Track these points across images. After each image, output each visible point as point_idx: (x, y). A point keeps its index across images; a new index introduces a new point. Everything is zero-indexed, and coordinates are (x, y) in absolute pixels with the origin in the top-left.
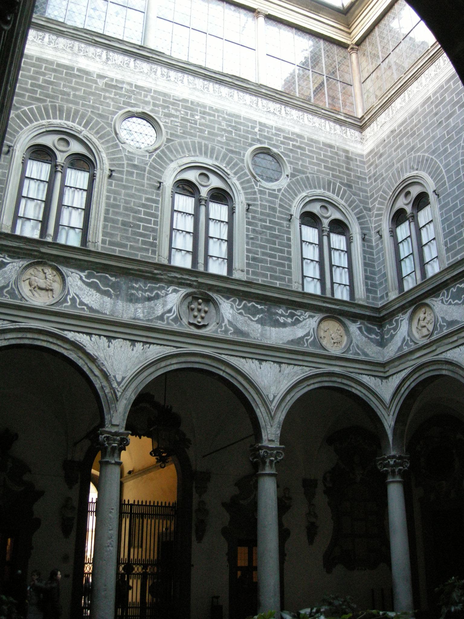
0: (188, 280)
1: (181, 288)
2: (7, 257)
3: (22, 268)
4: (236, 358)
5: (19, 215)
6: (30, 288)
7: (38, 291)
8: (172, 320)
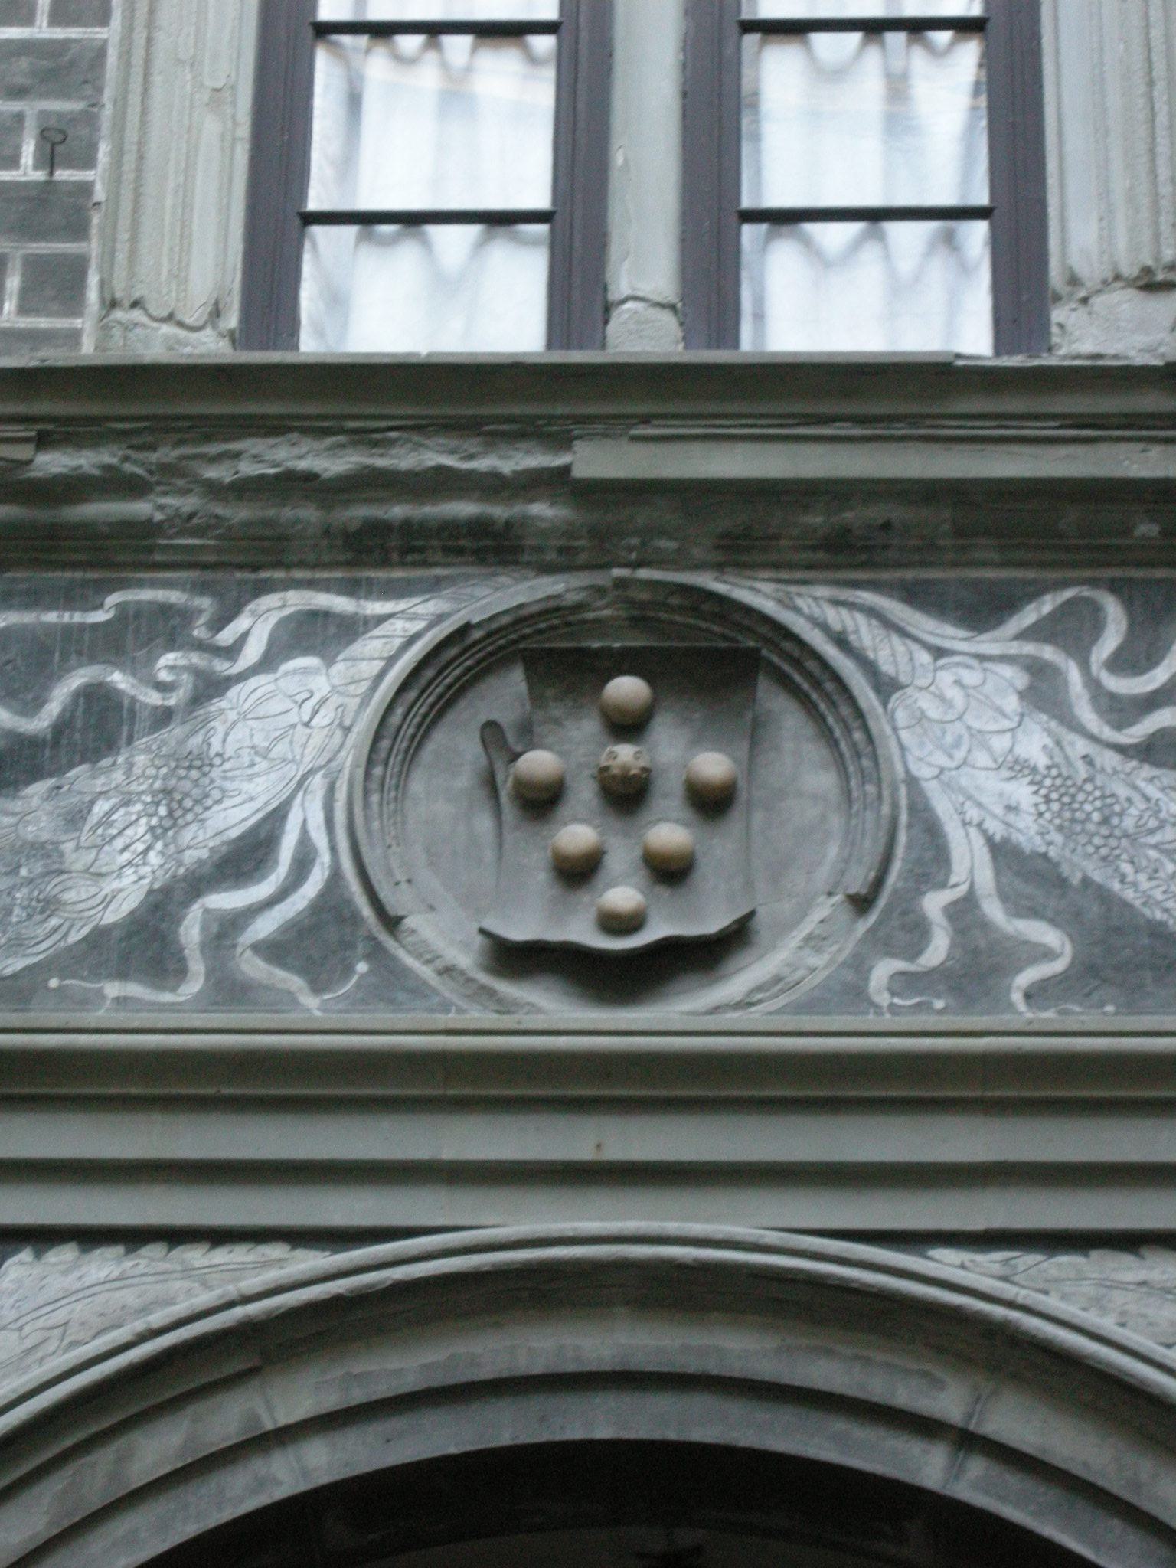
0: (442, 483)
1: (391, 591)
4: (1125, 1268)
8: (274, 950)
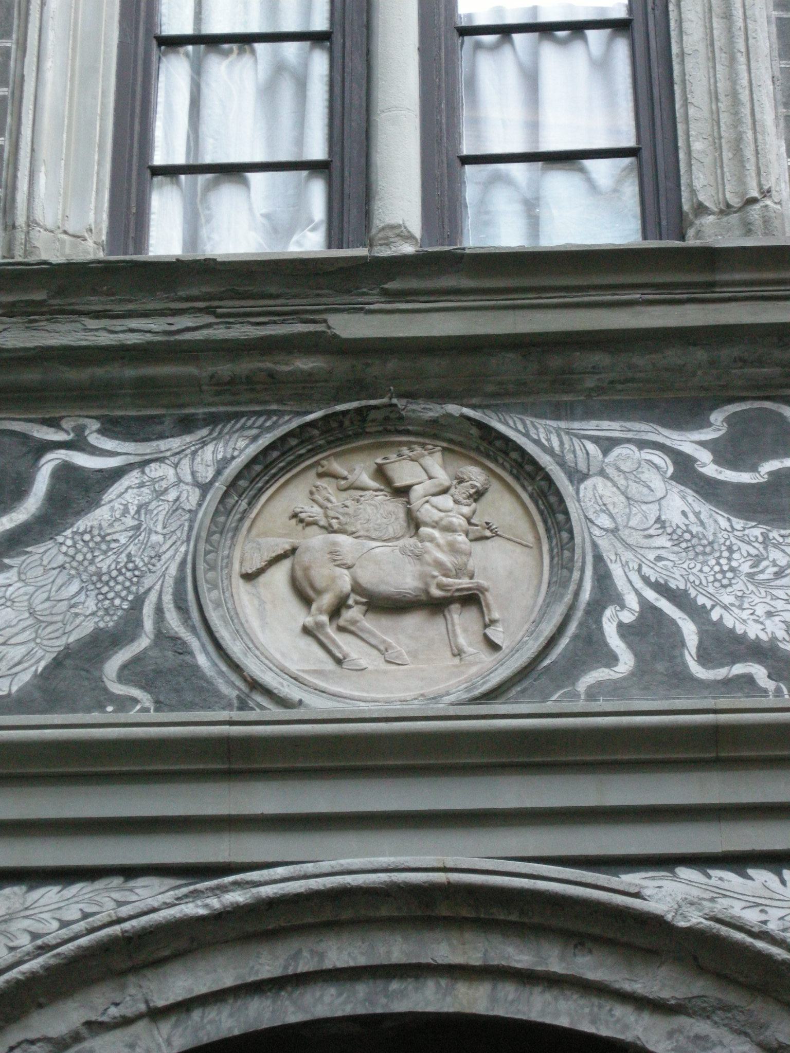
2: (95, 439)
3: (219, 487)
5: (159, 159)
6: (304, 618)
7: (370, 624)
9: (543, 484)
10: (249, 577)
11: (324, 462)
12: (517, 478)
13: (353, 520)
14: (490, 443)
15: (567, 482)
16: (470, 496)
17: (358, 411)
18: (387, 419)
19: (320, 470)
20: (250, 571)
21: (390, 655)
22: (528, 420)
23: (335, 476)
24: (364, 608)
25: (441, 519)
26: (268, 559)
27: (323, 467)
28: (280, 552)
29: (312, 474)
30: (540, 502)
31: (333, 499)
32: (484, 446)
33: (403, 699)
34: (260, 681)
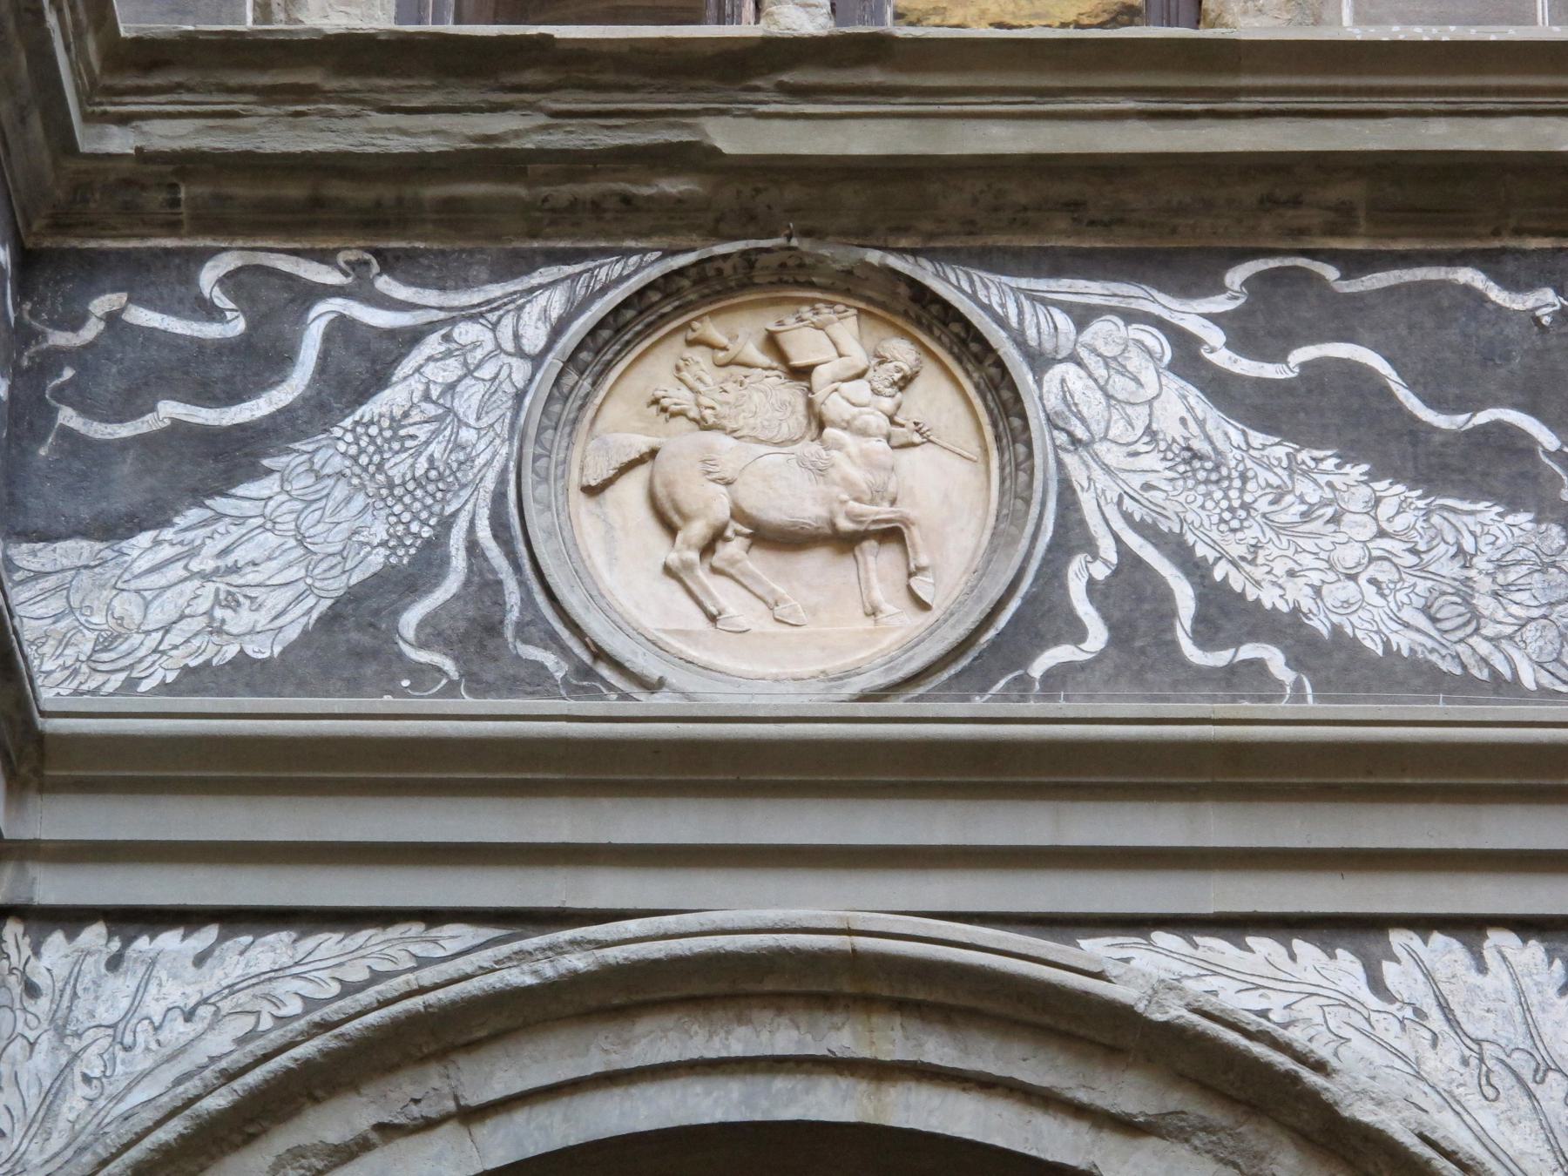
3: (553, 362)
7: (759, 565)
9: (993, 371)
10: (592, 491)
11: (696, 325)
12: (959, 360)
13: (733, 411)
14: (924, 307)
15: (1025, 368)
16: (894, 383)
17: (744, 254)
18: (783, 265)
19: (691, 335)
20: (593, 483)
21: (780, 611)
22: (977, 274)
23: (712, 346)
24: (747, 542)
25: (854, 418)
26: (618, 466)
27: (694, 330)
28: (634, 455)
29: (679, 340)
30: (989, 397)
31: (707, 379)
32: (915, 309)
33: (798, 676)
34: (607, 648)
